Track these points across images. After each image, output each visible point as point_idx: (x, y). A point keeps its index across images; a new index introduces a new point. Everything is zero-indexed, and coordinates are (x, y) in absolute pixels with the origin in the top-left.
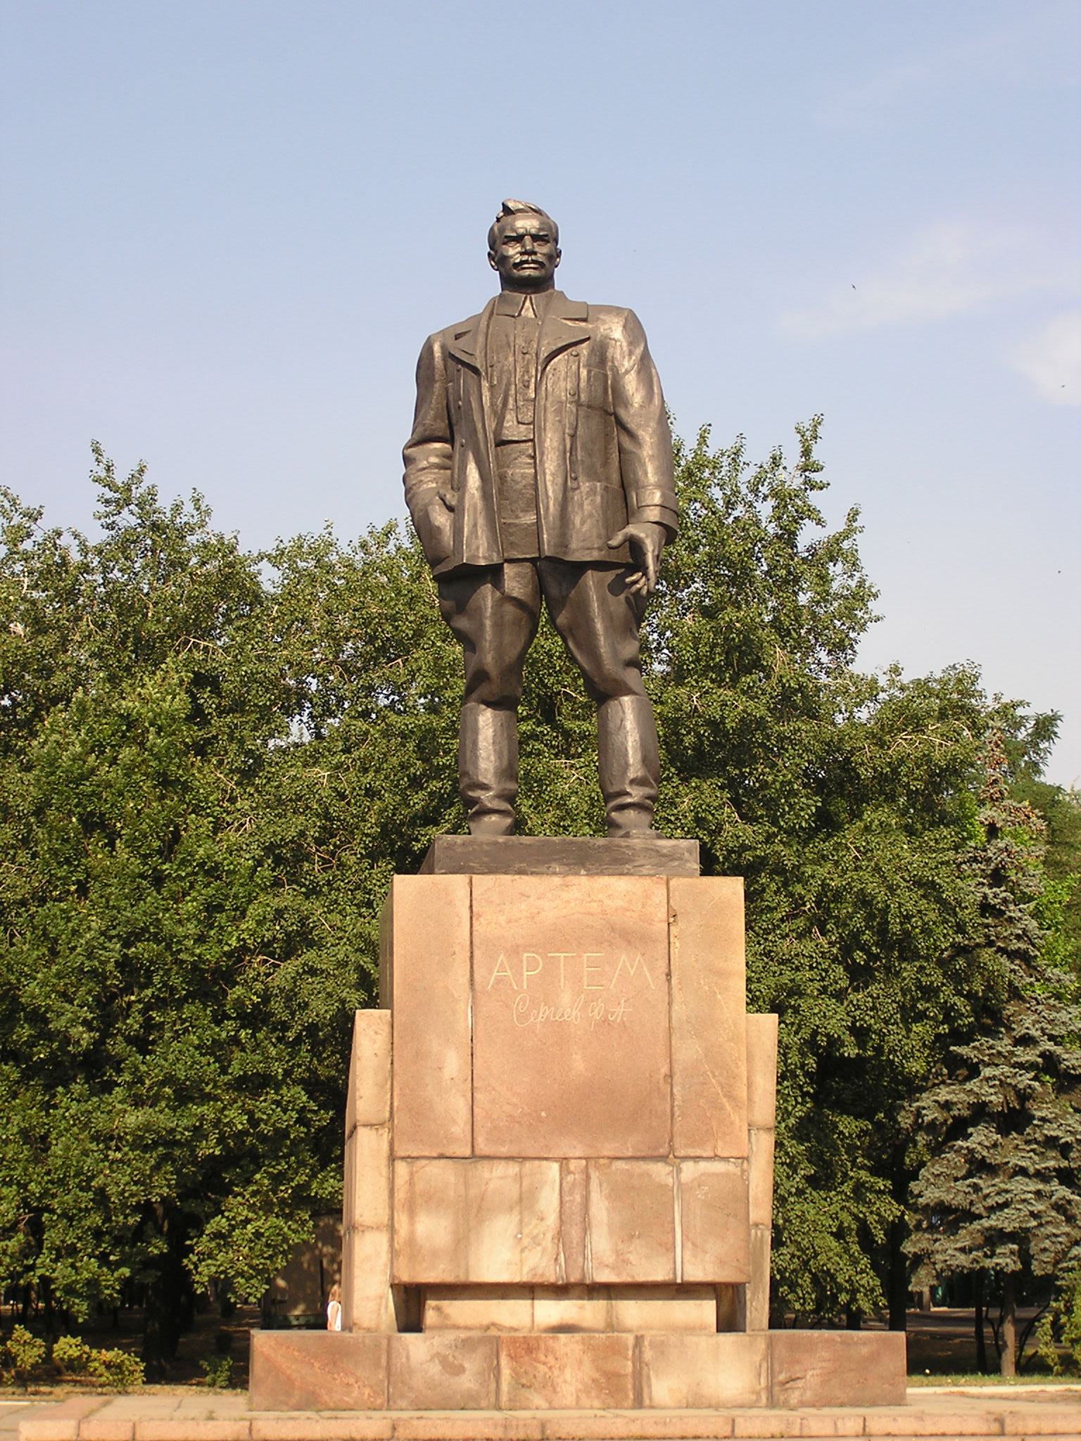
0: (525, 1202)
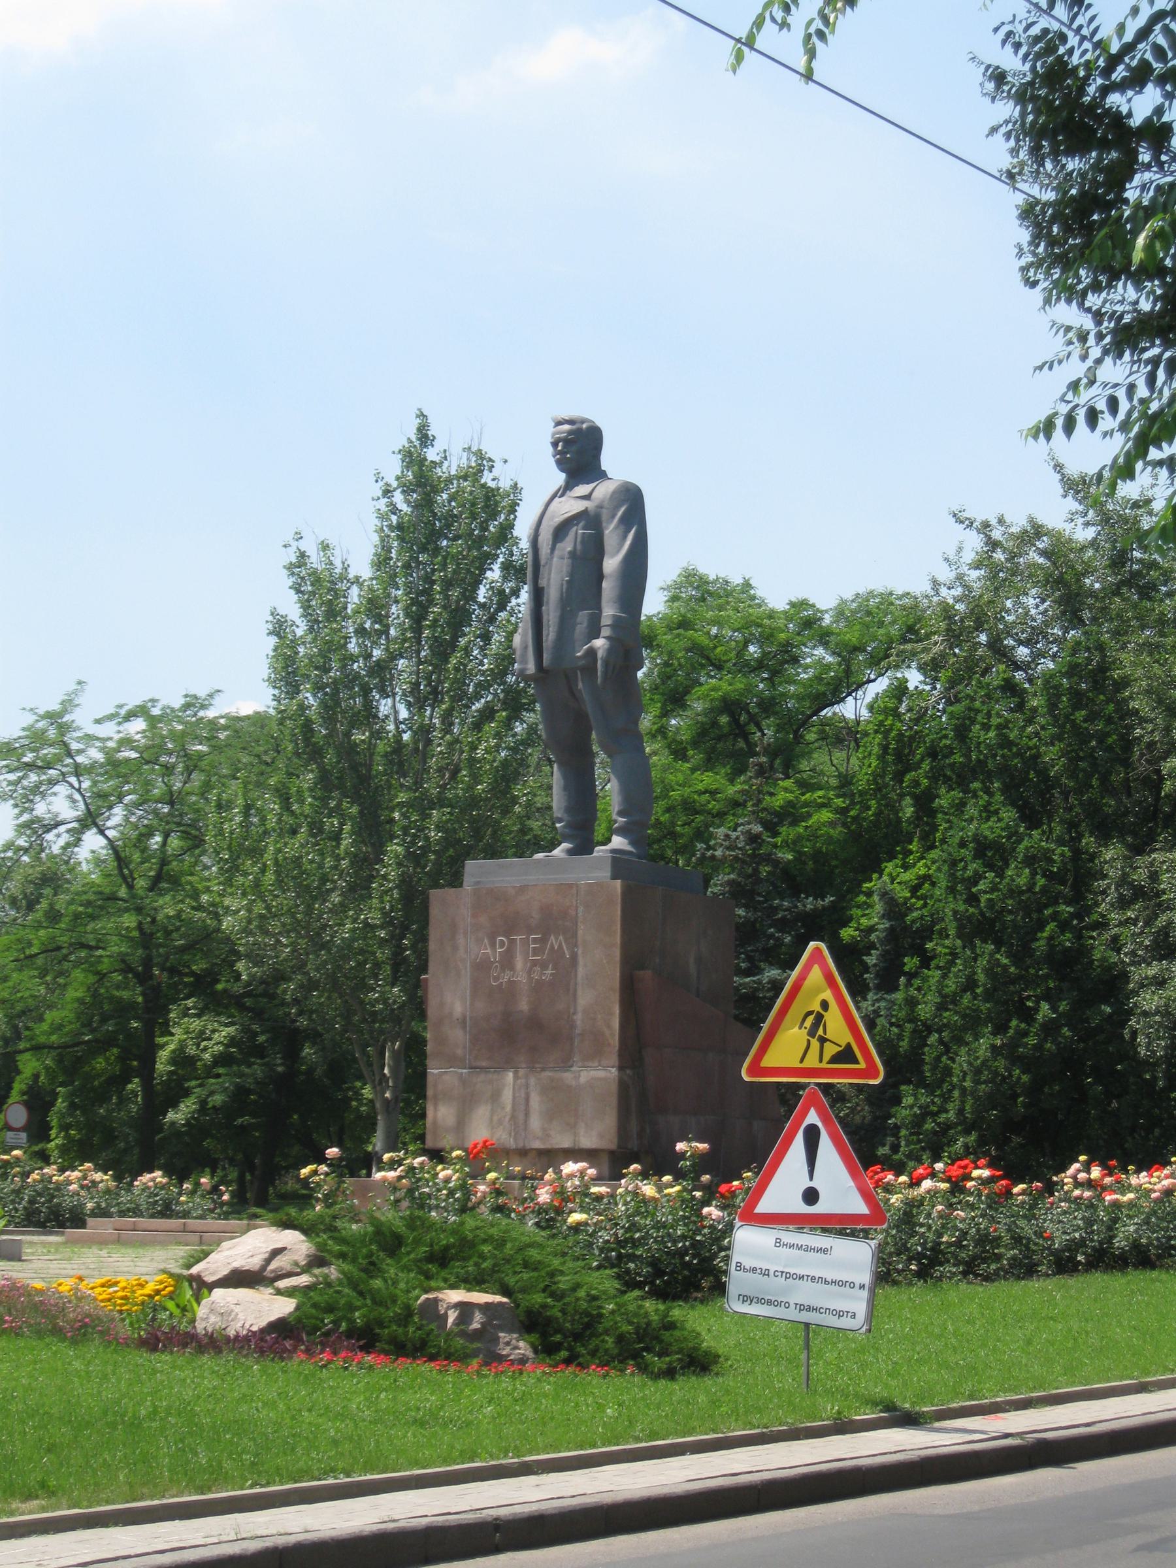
0: (495, 1097)
